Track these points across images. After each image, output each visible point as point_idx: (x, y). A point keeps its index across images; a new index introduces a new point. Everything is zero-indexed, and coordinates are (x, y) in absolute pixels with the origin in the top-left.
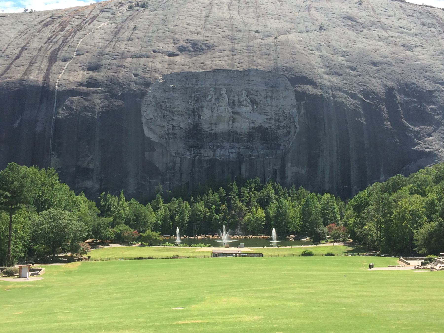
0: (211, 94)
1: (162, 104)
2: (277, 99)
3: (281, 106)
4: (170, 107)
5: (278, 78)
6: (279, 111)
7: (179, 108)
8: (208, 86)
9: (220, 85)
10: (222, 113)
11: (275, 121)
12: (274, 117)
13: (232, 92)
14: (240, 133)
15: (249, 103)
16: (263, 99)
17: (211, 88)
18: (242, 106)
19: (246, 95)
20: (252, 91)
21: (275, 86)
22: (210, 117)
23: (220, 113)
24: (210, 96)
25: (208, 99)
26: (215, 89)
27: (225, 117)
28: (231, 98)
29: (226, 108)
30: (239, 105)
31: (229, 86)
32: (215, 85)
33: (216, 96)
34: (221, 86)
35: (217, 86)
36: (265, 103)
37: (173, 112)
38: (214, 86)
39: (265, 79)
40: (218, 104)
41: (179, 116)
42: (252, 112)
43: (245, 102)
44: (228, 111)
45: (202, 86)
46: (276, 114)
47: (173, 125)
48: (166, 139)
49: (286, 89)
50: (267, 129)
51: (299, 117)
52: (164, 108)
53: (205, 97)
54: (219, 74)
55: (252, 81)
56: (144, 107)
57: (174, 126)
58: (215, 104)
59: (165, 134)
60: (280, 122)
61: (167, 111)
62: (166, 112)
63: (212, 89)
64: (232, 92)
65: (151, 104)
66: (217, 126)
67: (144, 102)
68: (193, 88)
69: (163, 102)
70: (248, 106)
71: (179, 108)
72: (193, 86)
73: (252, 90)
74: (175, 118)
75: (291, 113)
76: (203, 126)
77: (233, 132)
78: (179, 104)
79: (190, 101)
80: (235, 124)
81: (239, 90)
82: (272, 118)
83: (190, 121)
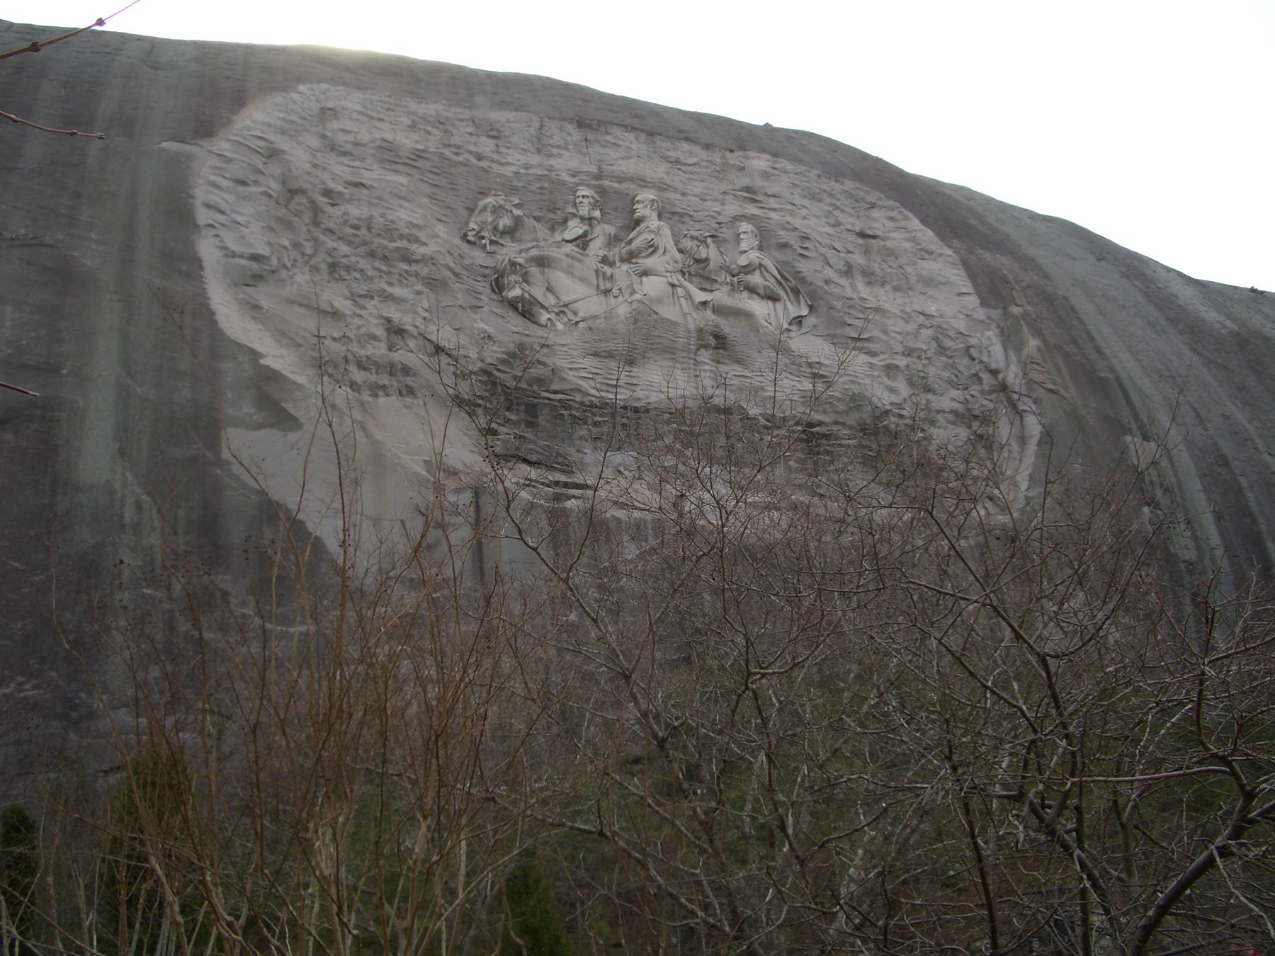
1: (321, 200)
2: (896, 289)
3: (921, 317)
4: (369, 229)
5: (873, 206)
6: (916, 335)
7: (417, 241)
10: (659, 301)
11: (911, 383)
12: (901, 362)
13: (687, 219)
14: (763, 421)
16: (830, 273)
18: (745, 294)
20: (781, 233)
21: (869, 232)
22: (595, 317)
23: (651, 300)
26: (602, 191)
27: (675, 324)
28: (687, 244)
31: (670, 195)
32: (598, 178)
33: (610, 229)
34: (626, 185)
35: (606, 183)
36: (848, 292)
37: (385, 258)
39: (820, 200)
41: (419, 287)
45: (530, 171)
46: (909, 353)
47: (388, 320)
48: (353, 386)
49: (922, 249)
50: (887, 412)
51: (1024, 365)
52: (331, 225)
53: (552, 229)
54: (608, 138)
55: (766, 195)
56: (218, 187)
57: (396, 331)
59: (347, 361)
60: (934, 392)
61: (350, 243)
62: (345, 249)
63: (583, 191)
65: (256, 183)
66: (636, 371)
67: (214, 161)
69: (327, 193)
71: (417, 241)
72: (484, 164)
73: (784, 229)
74: (397, 291)
75: (972, 351)
76: (560, 363)
77: (727, 411)
78: (421, 222)
80: (732, 370)
81: (720, 219)
82: (897, 367)
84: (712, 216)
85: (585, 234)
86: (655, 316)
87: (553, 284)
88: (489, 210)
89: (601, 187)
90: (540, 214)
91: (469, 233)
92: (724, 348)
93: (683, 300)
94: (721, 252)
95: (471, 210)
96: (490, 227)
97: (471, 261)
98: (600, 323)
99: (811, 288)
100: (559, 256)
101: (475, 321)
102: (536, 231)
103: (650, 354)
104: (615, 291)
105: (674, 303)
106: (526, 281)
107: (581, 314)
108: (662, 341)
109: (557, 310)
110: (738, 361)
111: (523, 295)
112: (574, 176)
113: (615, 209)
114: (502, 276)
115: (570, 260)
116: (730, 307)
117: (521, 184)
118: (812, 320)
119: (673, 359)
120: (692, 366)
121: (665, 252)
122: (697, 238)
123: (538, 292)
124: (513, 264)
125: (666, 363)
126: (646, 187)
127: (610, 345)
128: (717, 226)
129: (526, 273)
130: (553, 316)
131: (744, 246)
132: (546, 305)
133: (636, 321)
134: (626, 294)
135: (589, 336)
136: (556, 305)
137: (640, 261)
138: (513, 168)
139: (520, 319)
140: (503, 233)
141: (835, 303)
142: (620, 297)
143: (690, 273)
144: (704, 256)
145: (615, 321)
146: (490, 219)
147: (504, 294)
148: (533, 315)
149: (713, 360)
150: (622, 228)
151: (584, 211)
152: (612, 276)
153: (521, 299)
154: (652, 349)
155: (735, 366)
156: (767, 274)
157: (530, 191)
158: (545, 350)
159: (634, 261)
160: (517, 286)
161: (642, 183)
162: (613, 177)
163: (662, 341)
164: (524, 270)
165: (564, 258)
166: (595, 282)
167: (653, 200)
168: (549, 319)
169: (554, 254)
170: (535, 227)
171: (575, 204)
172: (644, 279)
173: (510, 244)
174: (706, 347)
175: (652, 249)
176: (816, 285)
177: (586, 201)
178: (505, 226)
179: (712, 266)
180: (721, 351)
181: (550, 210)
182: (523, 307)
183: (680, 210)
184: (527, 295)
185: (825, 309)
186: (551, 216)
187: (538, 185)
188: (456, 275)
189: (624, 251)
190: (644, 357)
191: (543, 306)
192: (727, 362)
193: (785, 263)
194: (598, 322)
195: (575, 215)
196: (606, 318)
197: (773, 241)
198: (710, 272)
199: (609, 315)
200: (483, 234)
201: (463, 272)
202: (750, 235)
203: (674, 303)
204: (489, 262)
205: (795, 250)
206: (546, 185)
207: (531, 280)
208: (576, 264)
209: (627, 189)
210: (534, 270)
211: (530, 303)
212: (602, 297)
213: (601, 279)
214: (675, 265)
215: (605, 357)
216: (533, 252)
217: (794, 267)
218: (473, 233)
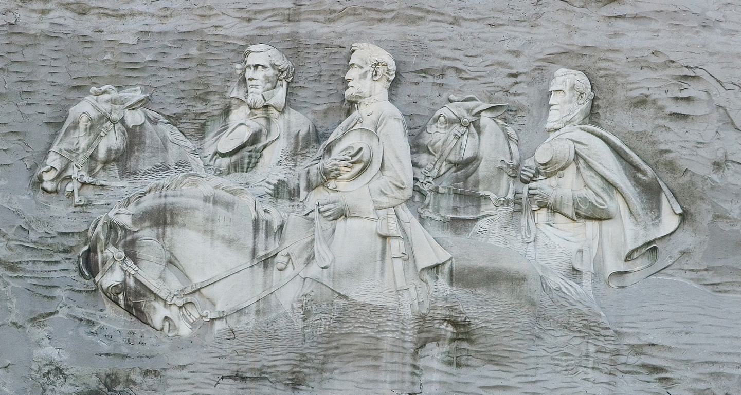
0: (256, 95)
8: (227, 22)
9: (343, 14)
10: (350, 274)
13: (451, 79)
15: (611, 185)
17: (252, 40)
18: (542, 215)
19: (585, 105)
22: (240, 311)
23: (335, 277)
24: (238, 115)
25: (227, 143)
27: (380, 310)
28: (437, 135)
29: (393, 228)
30: (518, 206)
31: (424, 30)
32: (292, 17)
34: (340, 26)
35: (306, 27)
38: (286, 29)
40: (319, 196)
42: (639, 265)
43: (571, 171)
44: (409, 257)
53: (201, 131)
58: (293, 195)
63: (261, 54)
64: (451, 79)
68: (85, 40)
70: (598, 216)
72: (86, 25)
73: (645, 65)
79: (54, 161)
81: (520, 65)
83: (49, 351)
84: (500, 64)
85: (255, 138)
86: (342, 303)
87: (178, 253)
88: (82, 126)
89: (294, 37)
90: (179, 110)
91: (47, 177)
92: (468, 340)
93: (399, 264)
94: (508, 137)
95: (56, 125)
96: (82, 159)
97: (41, 230)
98: (248, 322)
99: (686, 179)
100: (193, 202)
101: (38, 344)
102: (165, 148)
103: (336, 363)
104: (281, 259)
105: (382, 274)
106: (133, 257)
107: (220, 307)
108: (355, 340)
109: (180, 302)
110: (492, 360)
111: (125, 282)
112: (249, 20)
113: (318, 79)
114: (93, 250)
115: (210, 205)
116: (481, 270)
117: (149, 58)
118: (686, 239)
119: (376, 367)
120: (408, 377)
121: (382, 167)
122: (459, 121)
123: (149, 275)
124: (112, 227)
125: (363, 374)
126: (380, 20)
127: (263, 359)
128: (513, 80)
129: (133, 242)
130: (173, 313)
131: (553, 119)
132: (162, 295)
133: (307, 314)
134: (299, 263)
135: (228, 347)
136: (182, 293)
137: (341, 185)
138: (135, 25)
139: (124, 316)
140: (106, 163)
141: (727, 206)
142: (289, 271)
143: (436, 191)
144: (468, 154)
145: (274, 315)
146: (83, 144)
147: (97, 279)
148: (143, 313)
149: (450, 363)
150: (326, 112)
151: (256, 95)
152: (281, 227)
153: (123, 287)
154: (336, 355)
155: (489, 370)
156: (587, 173)
157: (168, 69)
158: (150, 380)
159: (332, 184)
160: (118, 265)
161: (374, 15)
162: (318, 13)
163: (355, 340)
164: (129, 238)
165: (200, 203)
166: (250, 244)
167: (377, 64)
168: (166, 318)
169: (183, 200)
170: (164, 140)
171: (244, 80)
172: (340, 224)
173: (120, 183)
174: (437, 339)
175: (359, 167)
176: (694, 174)
177: (260, 74)
178: (109, 151)
179: (483, 170)
180: (465, 345)
181: (198, 98)
182: (126, 300)
183: (438, 63)
184: (131, 282)
185: (710, 217)
186: (200, 107)
187: (180, 54)
188: (11, 267)
189: (314, 170)
190: (322, 371)
191: (157, 297)
192: (474, 362)
193: (640, 135)
194: (244, 319)
195: (243, 102)
196: (258, 312)
197: (621, 94)
198: (477, 184)
199: (263, 306)
200: (69, 172)
201: (27, 256)
202: (568, 95)
203: (382, 274)
204: (77, 224)
205: (661, 108)
206: (194, 52)
207: (141, 253)
208: (221, 210)
209: (340, 35)
210: (147, 234)
211: (138, 294)
212: (259, 270)
213: (262, 235)
214: (398, 194)
215: (254, 379)
216: (149, 202)
217: (653, 143)
218: (53, 174)
